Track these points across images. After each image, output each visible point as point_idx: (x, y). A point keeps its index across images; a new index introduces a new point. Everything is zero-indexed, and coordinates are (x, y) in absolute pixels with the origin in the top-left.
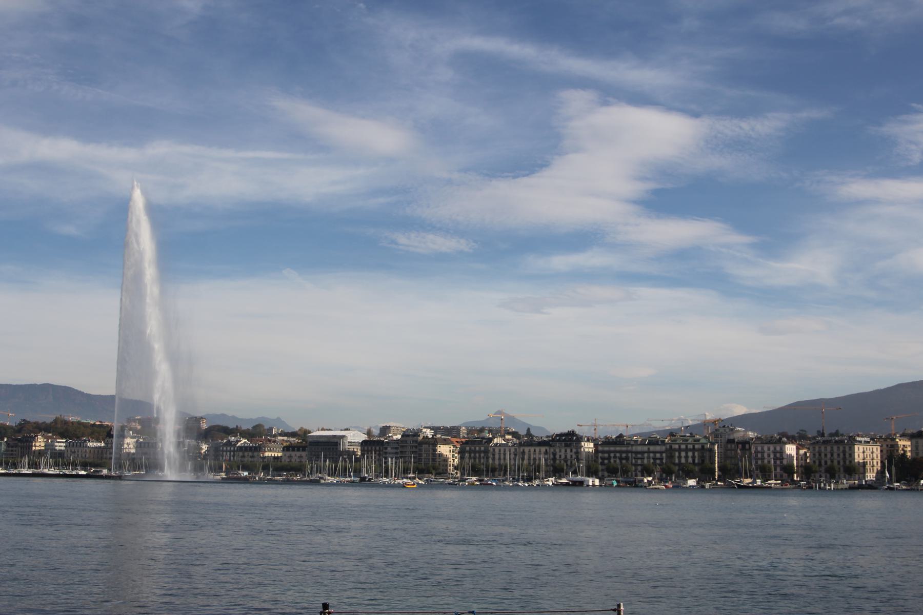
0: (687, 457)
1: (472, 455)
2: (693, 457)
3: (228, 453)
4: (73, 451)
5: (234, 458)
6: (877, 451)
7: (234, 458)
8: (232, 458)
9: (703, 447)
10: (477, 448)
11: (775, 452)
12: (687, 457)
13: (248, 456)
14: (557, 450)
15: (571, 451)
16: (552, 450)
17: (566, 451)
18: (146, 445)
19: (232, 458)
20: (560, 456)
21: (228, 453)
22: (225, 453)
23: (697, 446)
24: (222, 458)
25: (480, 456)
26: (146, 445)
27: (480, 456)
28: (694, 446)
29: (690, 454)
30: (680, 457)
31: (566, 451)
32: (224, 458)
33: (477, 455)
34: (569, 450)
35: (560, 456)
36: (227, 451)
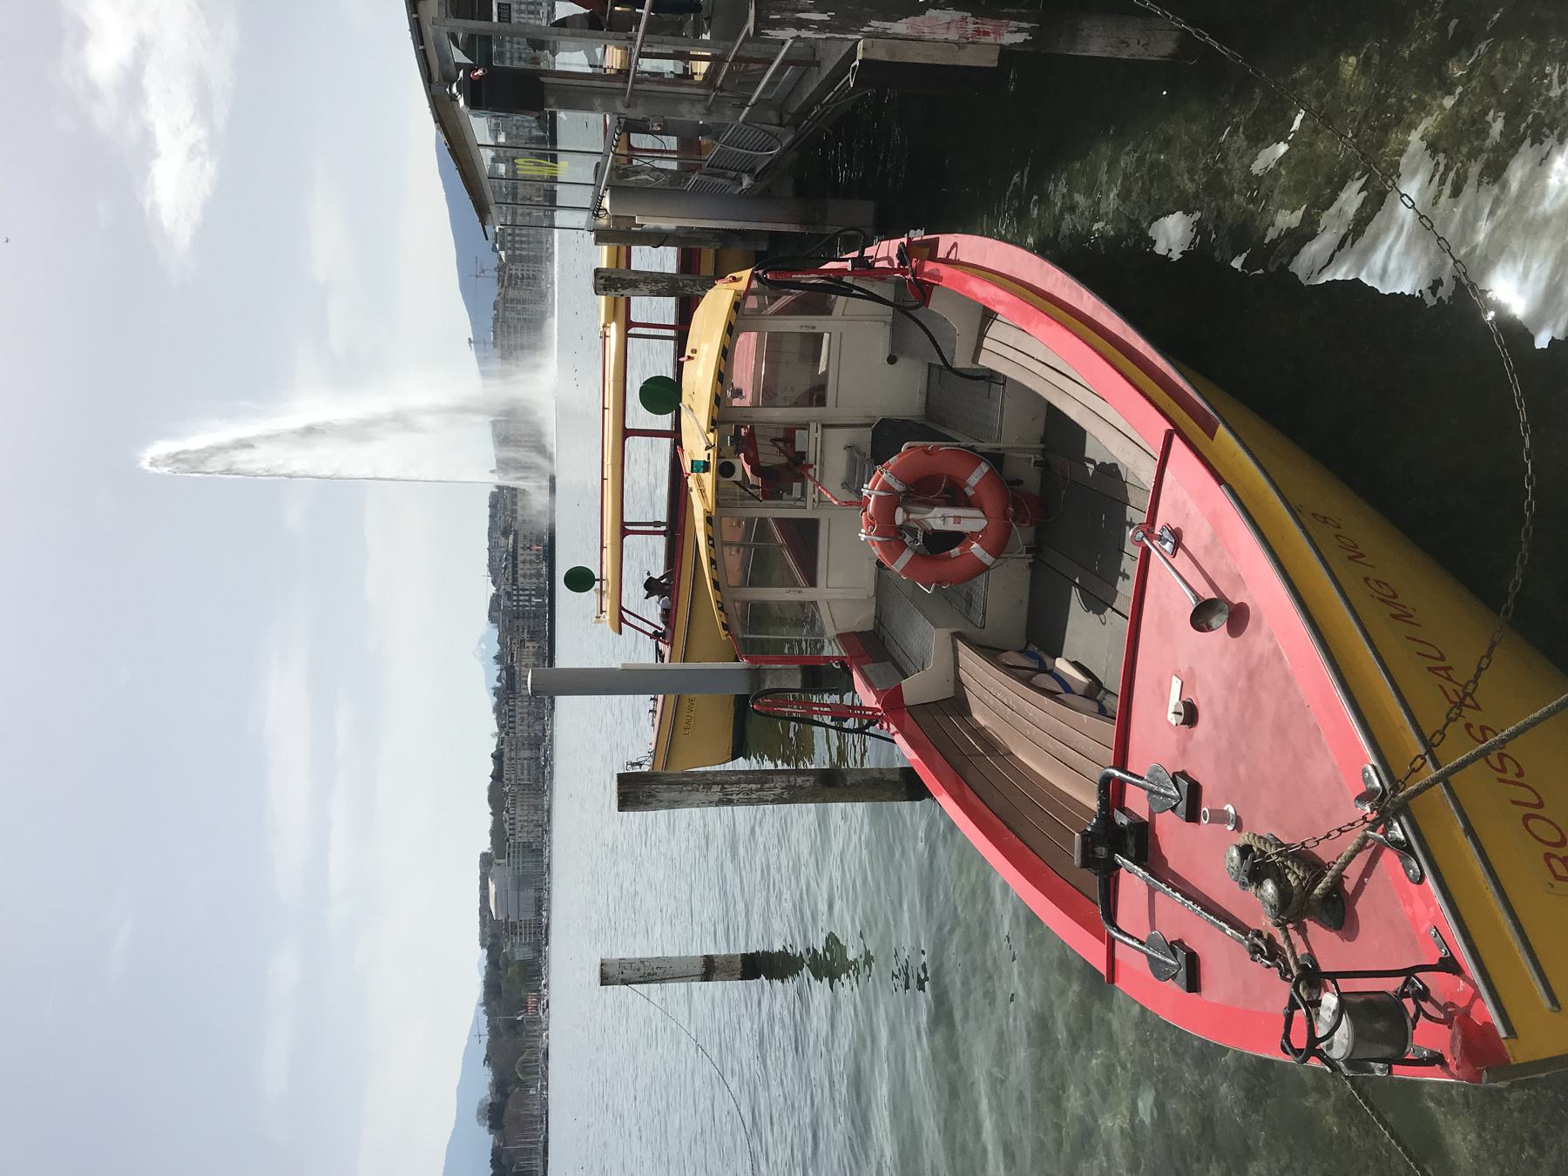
1: (517, 246)
3: (521, 598)
4: (519, 829)
5: (527, 590)
7: (527, 590)
8: (527, 592)
10: (509, 238)
13: (522, 569)
18: (511, 719)
19: (527, 592)
21: (521, 598)
22: (521, 603)
24: (527, 606)
25: (518, 235)
26: (511, 719)
27: (518, 235)
32: (527, 604)
33: (517, 238)
36: (518, 601)
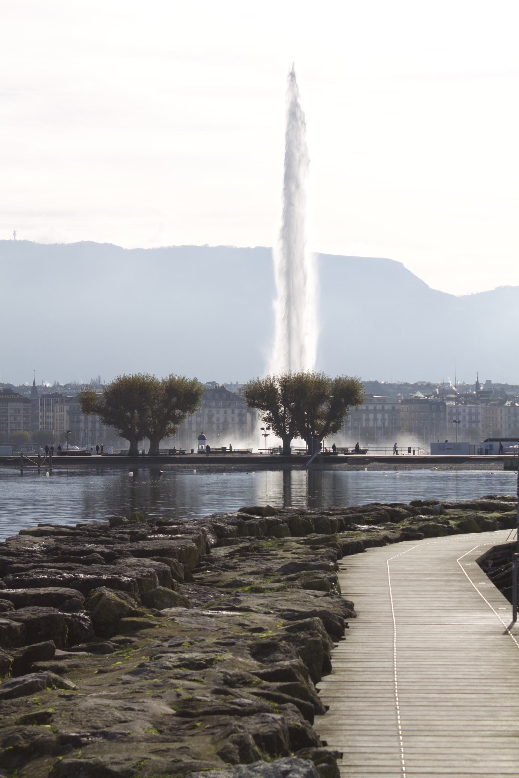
0: (375, 420)
2: (383, 420)
6: (501, 413)
9: (393, 408)
11: (470, 414)
12: (375, 420)
14: (214, 411)
15: (233, 412)
16: (207, 411)
17: (225, 412)
20: (218, 420)
23: (386, 407)
28: (383, 407)
29: (379, 416)
30: (367, 420)
31: (225, 412)
34: (229, 411)
35: (218, 420)
